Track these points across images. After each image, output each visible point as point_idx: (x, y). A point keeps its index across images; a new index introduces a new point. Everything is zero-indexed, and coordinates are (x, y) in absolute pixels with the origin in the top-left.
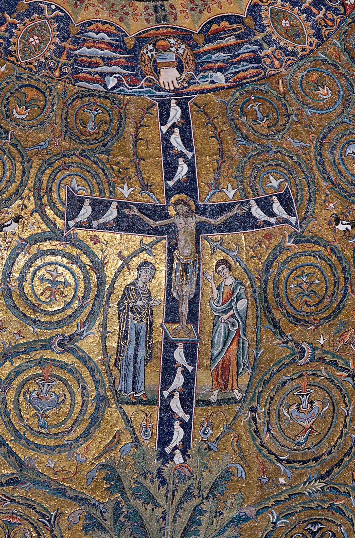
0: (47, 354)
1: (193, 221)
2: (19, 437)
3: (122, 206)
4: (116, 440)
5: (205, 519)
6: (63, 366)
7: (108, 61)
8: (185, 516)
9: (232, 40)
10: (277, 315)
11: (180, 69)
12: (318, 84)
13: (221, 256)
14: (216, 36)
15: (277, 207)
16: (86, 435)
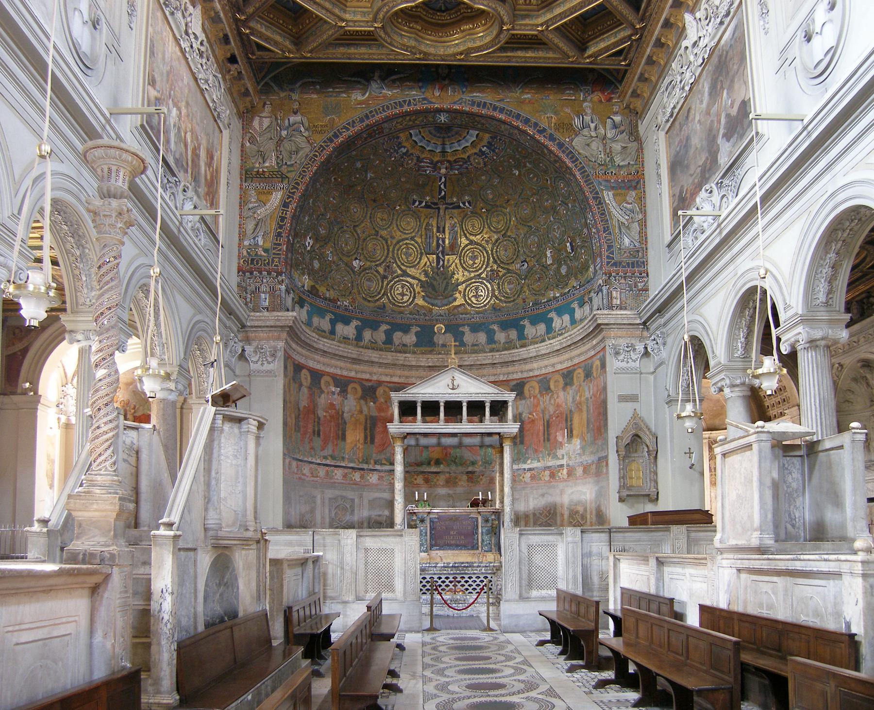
0: (408, 242)
1: (444, 206)
2: (403, 264)
3: (426, 202)
6: (412, 245)
7: (428, 167)
8: (445, 283)
9: (461, 163)
11: (446, 169)
13: (451, 215)
14: (457, 162)
15: (467, 204)
16: (419, 263)
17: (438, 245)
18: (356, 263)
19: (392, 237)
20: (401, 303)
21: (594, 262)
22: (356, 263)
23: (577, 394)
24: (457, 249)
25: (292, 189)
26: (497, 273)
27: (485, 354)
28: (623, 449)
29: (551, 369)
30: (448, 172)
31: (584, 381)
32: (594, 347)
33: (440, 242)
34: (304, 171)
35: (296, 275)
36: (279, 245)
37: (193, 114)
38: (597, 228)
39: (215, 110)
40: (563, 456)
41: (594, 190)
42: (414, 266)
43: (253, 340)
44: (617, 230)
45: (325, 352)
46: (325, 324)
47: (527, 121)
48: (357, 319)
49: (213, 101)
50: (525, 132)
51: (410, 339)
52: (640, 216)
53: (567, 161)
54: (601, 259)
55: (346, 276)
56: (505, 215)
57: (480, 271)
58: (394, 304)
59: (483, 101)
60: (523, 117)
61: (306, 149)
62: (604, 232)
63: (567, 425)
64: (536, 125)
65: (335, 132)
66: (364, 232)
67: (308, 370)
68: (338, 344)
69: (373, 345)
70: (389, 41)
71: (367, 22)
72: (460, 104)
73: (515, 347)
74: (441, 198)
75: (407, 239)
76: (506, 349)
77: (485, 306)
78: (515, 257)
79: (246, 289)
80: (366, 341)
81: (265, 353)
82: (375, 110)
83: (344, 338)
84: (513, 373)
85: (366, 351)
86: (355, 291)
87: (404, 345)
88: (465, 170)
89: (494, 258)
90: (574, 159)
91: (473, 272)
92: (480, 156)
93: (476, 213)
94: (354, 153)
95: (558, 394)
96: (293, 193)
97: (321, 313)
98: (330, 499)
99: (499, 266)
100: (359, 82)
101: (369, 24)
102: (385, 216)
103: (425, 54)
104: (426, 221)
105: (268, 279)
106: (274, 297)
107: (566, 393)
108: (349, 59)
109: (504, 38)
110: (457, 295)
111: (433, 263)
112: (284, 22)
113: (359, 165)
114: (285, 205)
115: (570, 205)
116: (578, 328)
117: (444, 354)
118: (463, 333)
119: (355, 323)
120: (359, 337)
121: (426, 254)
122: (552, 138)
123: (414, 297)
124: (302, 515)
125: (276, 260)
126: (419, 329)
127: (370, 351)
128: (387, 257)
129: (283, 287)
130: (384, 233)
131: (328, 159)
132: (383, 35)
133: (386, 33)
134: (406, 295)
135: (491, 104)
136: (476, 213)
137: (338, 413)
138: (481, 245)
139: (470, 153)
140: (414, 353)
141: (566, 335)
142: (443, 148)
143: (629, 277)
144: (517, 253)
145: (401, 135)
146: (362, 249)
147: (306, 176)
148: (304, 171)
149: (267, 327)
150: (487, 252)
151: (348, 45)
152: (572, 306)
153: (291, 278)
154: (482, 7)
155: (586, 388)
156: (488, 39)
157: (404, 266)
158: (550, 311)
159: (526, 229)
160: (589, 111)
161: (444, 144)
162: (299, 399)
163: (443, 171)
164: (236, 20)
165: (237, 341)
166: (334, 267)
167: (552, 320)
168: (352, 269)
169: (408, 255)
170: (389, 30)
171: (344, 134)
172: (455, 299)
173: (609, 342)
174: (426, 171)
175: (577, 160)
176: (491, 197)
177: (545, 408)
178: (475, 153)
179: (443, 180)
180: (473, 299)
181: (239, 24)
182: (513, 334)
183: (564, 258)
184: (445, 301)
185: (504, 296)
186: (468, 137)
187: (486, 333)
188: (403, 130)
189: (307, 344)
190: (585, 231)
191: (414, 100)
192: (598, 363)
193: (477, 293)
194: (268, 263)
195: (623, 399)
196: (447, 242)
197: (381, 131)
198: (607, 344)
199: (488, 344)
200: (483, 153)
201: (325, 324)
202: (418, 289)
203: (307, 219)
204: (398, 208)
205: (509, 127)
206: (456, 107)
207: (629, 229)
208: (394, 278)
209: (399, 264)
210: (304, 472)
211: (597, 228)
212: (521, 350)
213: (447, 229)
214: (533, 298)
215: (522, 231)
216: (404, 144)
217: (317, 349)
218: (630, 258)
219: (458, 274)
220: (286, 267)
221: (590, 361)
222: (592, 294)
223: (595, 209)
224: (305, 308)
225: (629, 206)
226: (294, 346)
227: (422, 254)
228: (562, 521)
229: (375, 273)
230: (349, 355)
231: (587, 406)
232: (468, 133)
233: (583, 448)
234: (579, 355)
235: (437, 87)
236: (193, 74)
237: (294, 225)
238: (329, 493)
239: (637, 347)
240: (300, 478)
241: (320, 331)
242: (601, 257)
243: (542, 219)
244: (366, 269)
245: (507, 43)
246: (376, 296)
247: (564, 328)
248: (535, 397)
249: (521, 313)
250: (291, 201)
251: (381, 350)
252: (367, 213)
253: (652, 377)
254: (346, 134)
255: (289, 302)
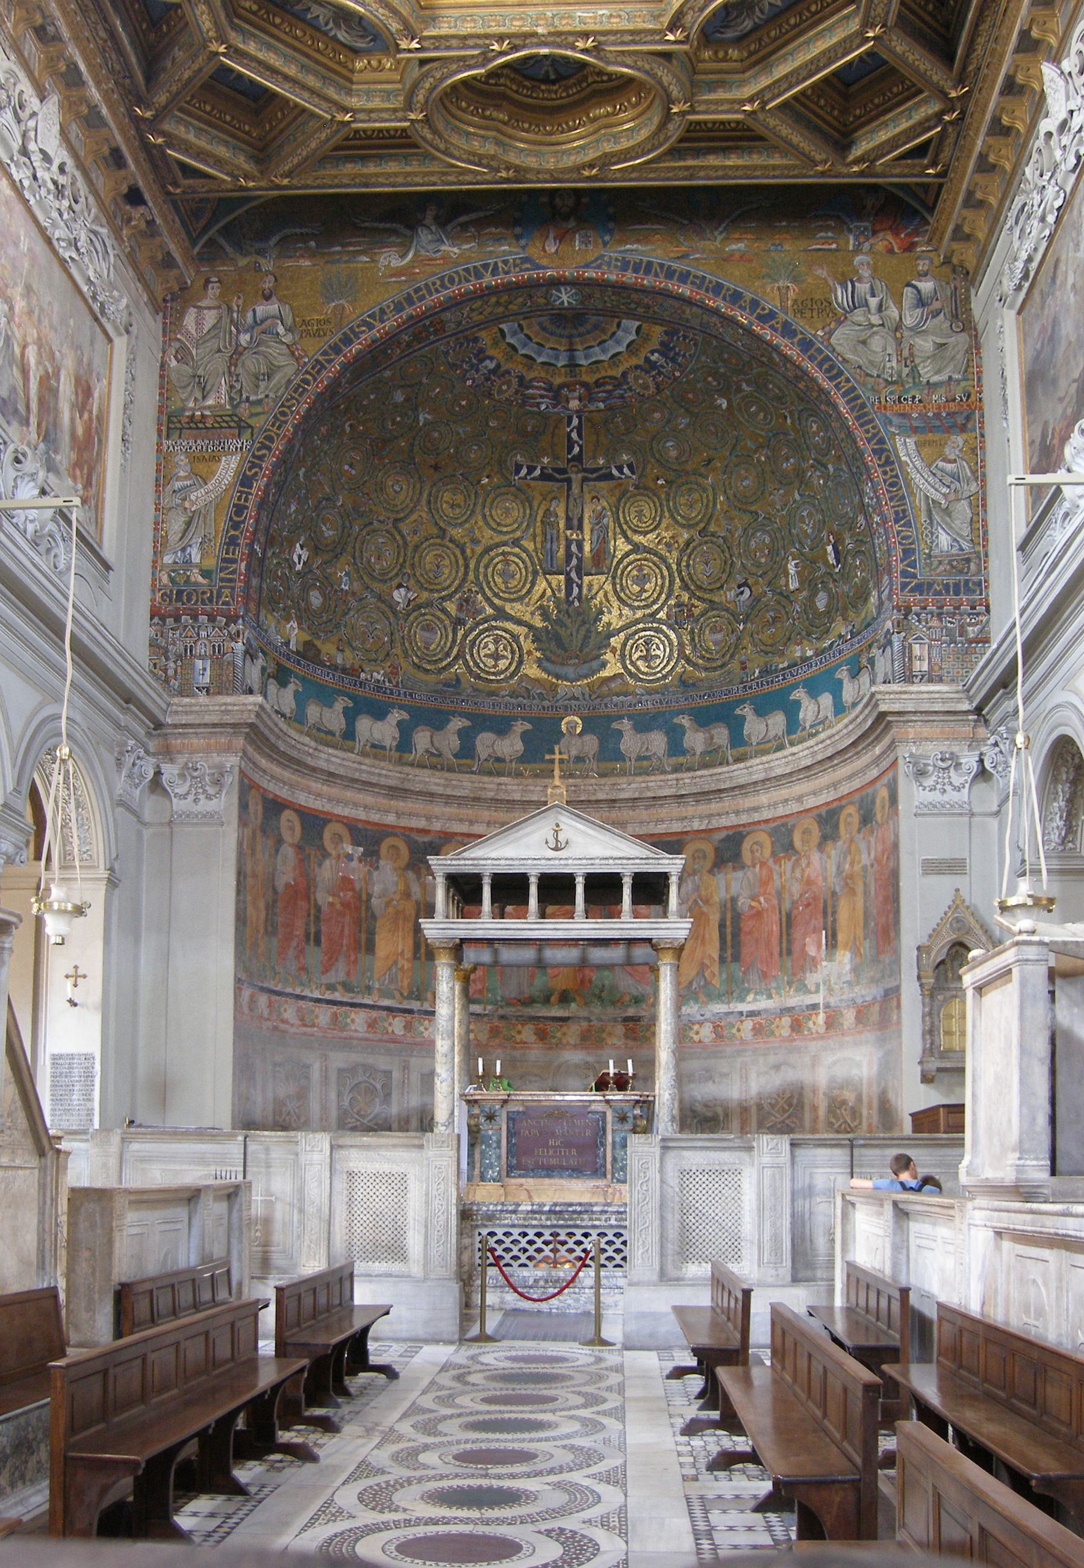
0: (507, 549)
1: (580, 475)
3: (542, 469)
4: (544, 591)
5: (593, 634)
7: (542, 397)
8: (582, 632)
9: (609, 387)
10: (625, 527)
11: (580, 400)
12: (654, 411)
14: (603, 384)
15: (626, 470)
16: (529, 592)
17: (569, 556)
18: (399, 595)
19: (475, 541)
20: (494, 674)
21: (878, 584)
22: (399, 595)
23: (845, 858)
24: (608, 562)
25: (259, 449)
26: (690, 610)
27: (662, 777)
28: (930, 973)
29: (795, 807)
30: (585, 406)
31: (859, 831)
32: (877, 761)
33: (574, 548)
34: (283, 414)
35: (270, 621)
36: (234, 561)
37: (42, 309)
38: (881, 514)
39: (94, 298)
40: (818, 986)
41: (875, 435)
42: (520, 599)
43: (179, 752)
44: (923, 518)
45: (331, 774)
46: (334, 718)
47: (736, 298)
48: (401, 707)
49: (89, 281)
50: (732, 321)
51: (511, 746)
52: (974, 487)
53: (819, 376)
54: (891, 579)
55: (377, 622)
56: (705, 490)
57: (655, 607)
58: (478, 677)
59: (645, 259)
60: (728, 289)
61: (288, 369)
62: (896, 521)
63: (825, 923)
64: (755, 304)
65: (345, 334)
66: (415, 533)
67: (296, 810)
68: (359, 758)
69: (434, 760)
70: (442, 146)
71: (395, 110)
72: (599, 267)
73: (724, 762)
74: (574, 459)
75: (505, 544)
76: (706, 766)
77: (665, 677)
78: (724, 576)
79: (166, 651)
80: (420, 751)
81: (202, 777)
82: (426, 285)
83: (374, 746)
84: (719, 815)
85: (417, 771)
86: (398, 650)
87: (499, 760)
88: (619, 402)
89: (682, 580)
90: (835, 372)
91: (639, 608)
92: (647, 372)
93: (646, 488)
94: (387, 374)
95: (808, 858)
96: (261, 458)
97: (326, 697)
98: (340, 1071)
99: (693, 595)
100: (394, 232)
101: (399, 115)
102: (459, 499)
103: (518, 169)
104: (543, 507)
105: (210, 630)
106: (221, 666)
107: (825, 857)
108: (366, 185)
109: (675, 130)
110: (609, 656)
111: (560, 591)
112: (233, 118)
113: (399, 397)
114: (245, 481)
115: (830, 467)
116: (846, 721)
117: (581, 777)
118: (620, 734)
119: (396, 716)
120: (405, 744)
121: (545, 573)
122: (788, 331)
123: (521, 662)
124: (279, 1104)
125: (227, 591)
126: (529, 726)
127: (427, 772)
128: (464, 580)
129: (239, 647)
130: (456, 532)
131: (335, 383)
132: (429, 136)
133: (435, 132)
134: (504, 657)
135: (661, 266)
136: (646, 488)
137: (360, 897)
138: (656, 554)
139: (627, 365)
140: (519, 775)
141: (822, 736)
142: (572, 358)
143: (948, 613)
144: (728, 567)
145: (483, 334)
146: (413, 566)
147: (286, 422)
148: (283, 414)
149: (206, 725)
150: (669, 568)
151: (364, 159)
152: (838, 676)
153: (258, 626)
154: (625, 70)
155: (863, 846)
156: (644, 134)
157: (500, 598)
158: (795, 687)
159: (747, 518)
160: (866, 273)
161: (571, 350)
162: (275, 869)
163: (574, 404)
164: (136, 120)
165: (142, 753)
166: (353, 603)
167: (797, 704)
168: (391, 607)
169: (506, 575)
170: (440, 126)
171: (363, 336)
172: (604, 665)
173: (904, 752)
174: (538, 405)
175: (840, 373)
176: (673, 453)
177: (783, 887)
178: (637, 367)
179: (575, 422)
180: (640, 663)
181: (142, 127)
182: (721, 735)
183: (822, 576)
184: (584, 669)
185: (703, 657)
186: (620, 333)
187: (667, 733)
188: (481, 325)
189: (291, 759)
190: (861, 519)
191: (505, 262)
192: (884, 793)
193: (648, 650)
194: (210, 600)
195: (934, 867)
196: (587, 548)
197: (439, 327)
198: (899, 754)
199: (669, 756)
200: (653, 365)
201: (334, 718)
202: (527, 645)
203: (293, 508)
204: (485, 481)
205: (700, 311)
206: (590, 274)
207: (949, 516)
208: (478, 624)
209: (489, 594)
210: (286, 1016)
211: (881, 514)
212: (735, 767)
213: (586, 521)
214: (762, 660)
215: (739, 524)
216: (491, 352)
217: (314, 769)
218: (950, 574)
219: (610, 612)
220: (246, 605)
221: (870, 790)
222: (875, 651)
223: (878, 475)
224: (291, 687)
225: (949, 467)
226: (263, 762)
227: (535, 573)
228: (815, 1120)
229: (439, 613)
230: (383, 781)
231: (865, 884)
232: (619, 325)
233: (856, 970)
234: (850, 777)
235: (551, 236)
236: (42, 230)
237: (264, 520)
238: (339, 1059)
239: (963, 761)
240: (275, 1028)
241: (323, 735)
242: (890, 573)
243: (777, 497)
244: (420, 607)
245: (681, 140)
246: (441, 660)
247: (822, 722)
248: (763, 864)
249: (737, 690)
250: (256, 474)
251: (450, 770)
252: (421, 494)
253: (994, 823)
254: (367, 336)
255: (253, 673)
